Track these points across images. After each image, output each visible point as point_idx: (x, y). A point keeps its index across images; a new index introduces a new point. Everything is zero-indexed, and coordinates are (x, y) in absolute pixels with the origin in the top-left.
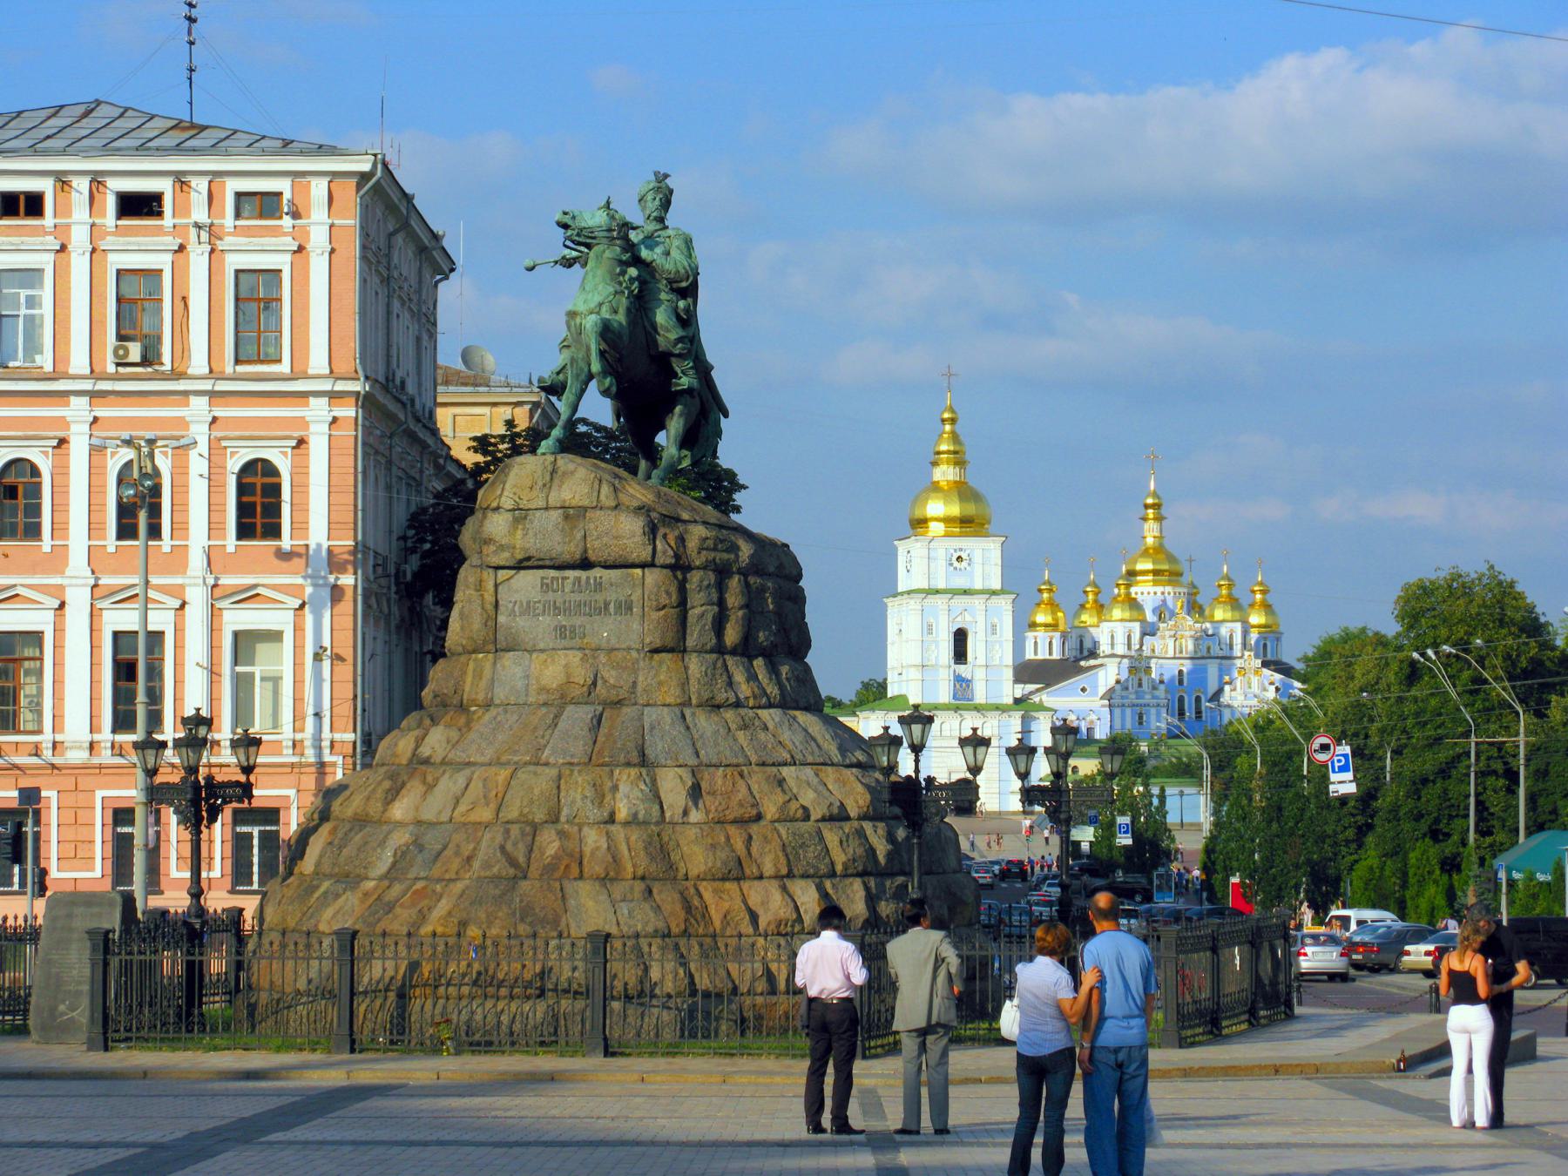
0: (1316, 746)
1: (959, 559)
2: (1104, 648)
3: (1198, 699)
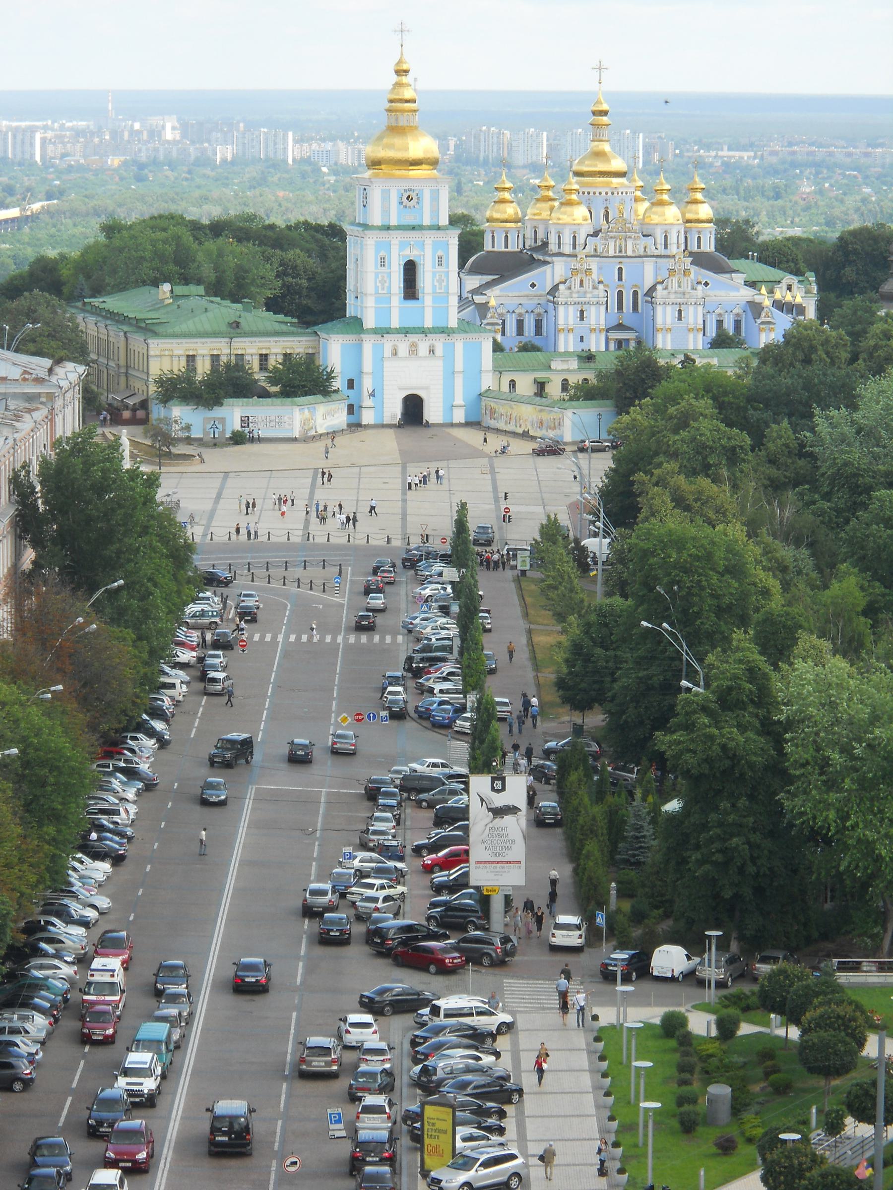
0: (288, 1162)
2: (553, 247)
3: (635, 293)
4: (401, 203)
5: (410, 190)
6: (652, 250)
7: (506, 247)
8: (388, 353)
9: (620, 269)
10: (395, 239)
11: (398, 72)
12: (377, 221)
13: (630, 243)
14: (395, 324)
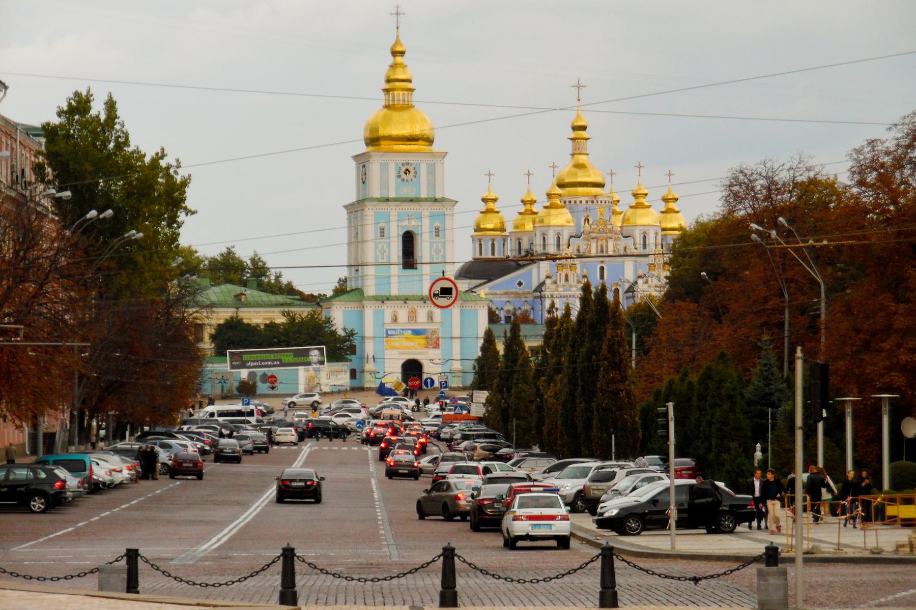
1: (407, 171)
4: (399, 176)
5: (408, 164)
6: (631, 250)
7: (493, 253)
8: (388, 318)
9: (602, 269)
10: (394, 211)
11: (395, 53)
12: (377, 194)
13: (611, 244)
14: (394, 292)
